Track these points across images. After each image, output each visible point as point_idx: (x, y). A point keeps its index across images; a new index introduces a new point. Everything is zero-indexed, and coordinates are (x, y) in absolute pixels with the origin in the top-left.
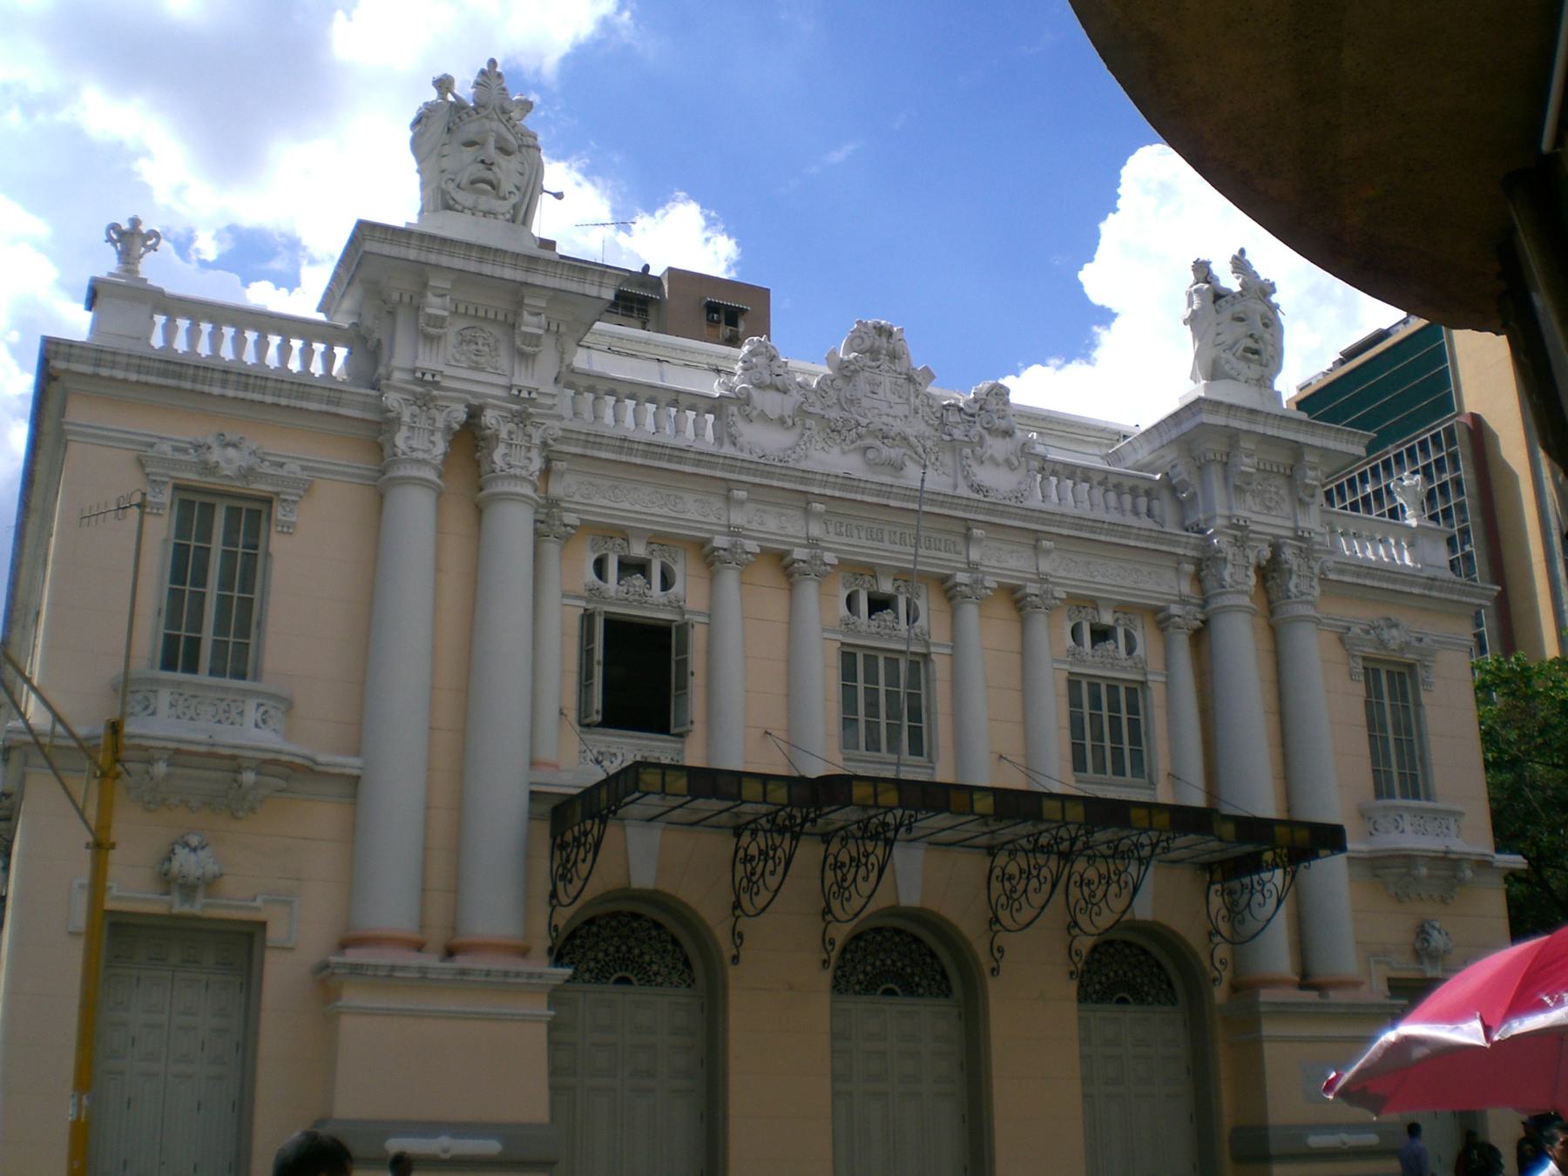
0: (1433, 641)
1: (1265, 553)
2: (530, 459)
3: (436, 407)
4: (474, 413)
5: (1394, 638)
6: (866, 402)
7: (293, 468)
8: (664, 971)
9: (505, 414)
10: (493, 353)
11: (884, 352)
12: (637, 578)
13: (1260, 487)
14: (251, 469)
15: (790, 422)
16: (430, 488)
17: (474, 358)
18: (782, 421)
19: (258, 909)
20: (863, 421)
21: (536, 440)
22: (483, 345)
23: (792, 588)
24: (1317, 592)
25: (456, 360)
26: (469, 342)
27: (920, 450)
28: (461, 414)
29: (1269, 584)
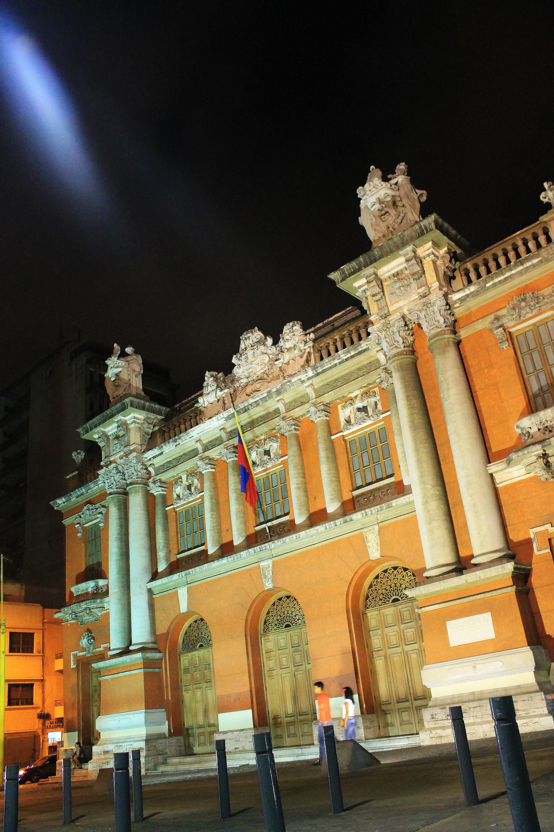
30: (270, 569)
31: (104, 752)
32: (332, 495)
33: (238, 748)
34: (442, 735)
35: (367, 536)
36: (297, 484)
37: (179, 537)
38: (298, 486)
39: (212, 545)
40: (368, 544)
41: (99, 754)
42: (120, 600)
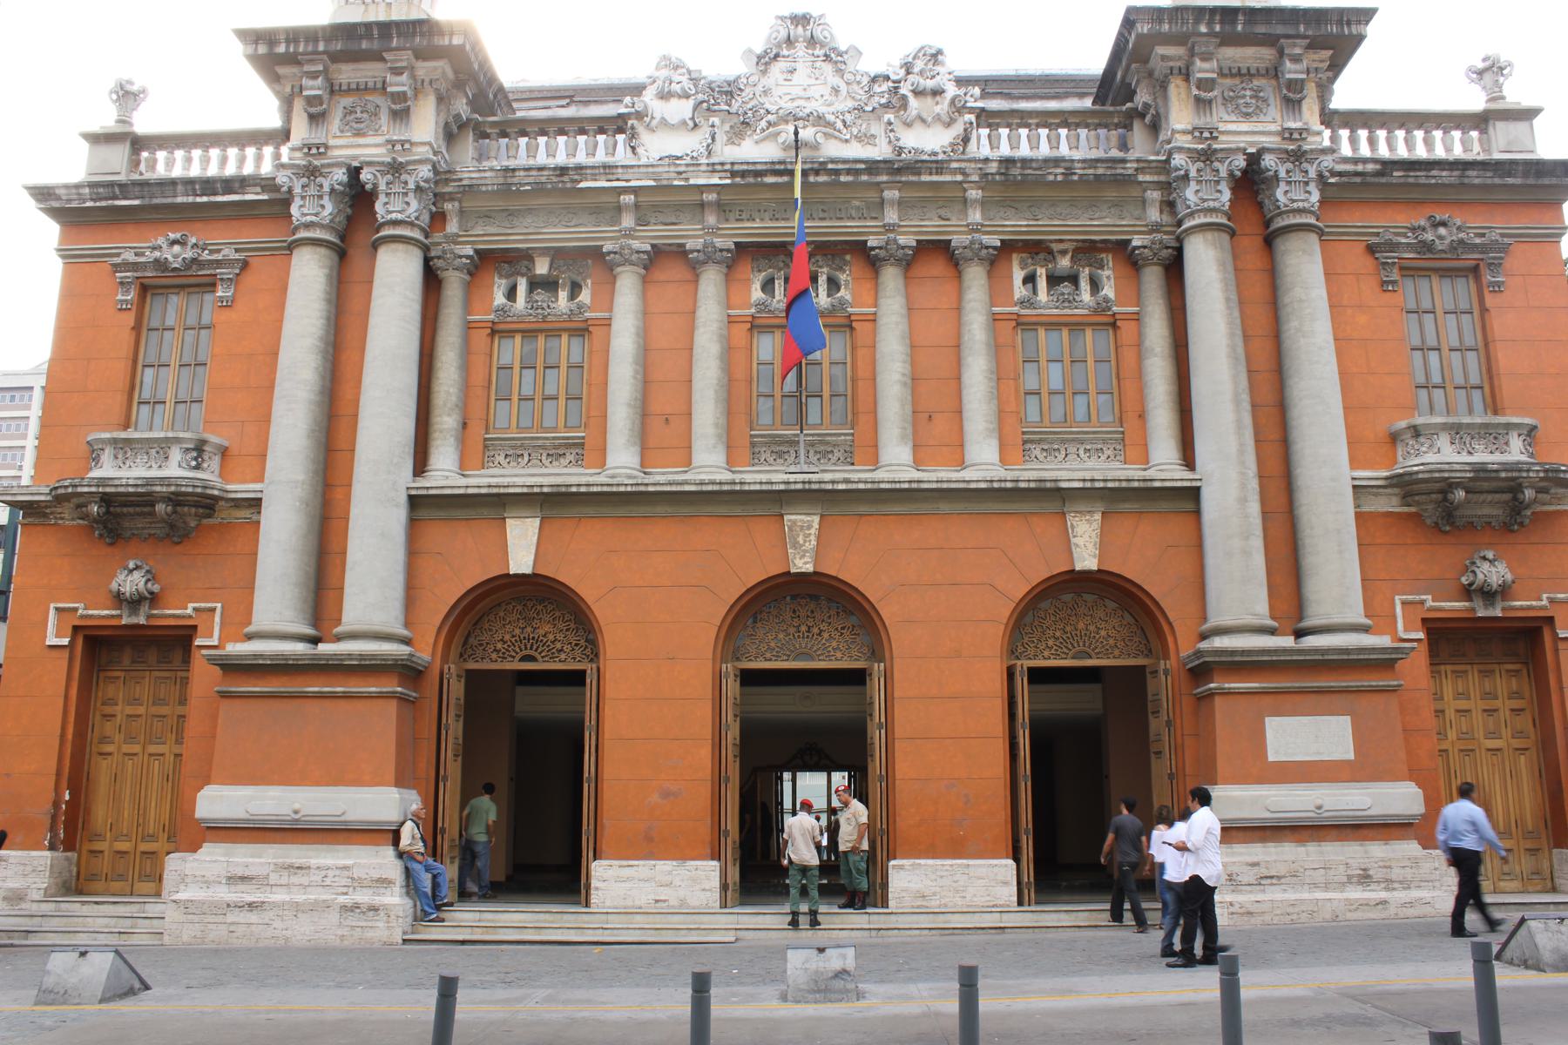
0: (1503, 235)
1: (1237, 163)
2: (408, 204)
3: (321, 175)
4: (354, 172)
5: (1441, 238)
6: (777, 92)
7: (229, 253)
8: (567, 648)
9: (382, 168)
10: (373, 118)
11: (801, 39)
12: (538, 294)
13: (1231, 94)
14: (194, 260)
15: (691, 124)
16: (321, 245)
17: (355, 126)
18: (684, 123)
19: (190, 617)
20: (773, 108)
21: (412, 186)
22: (362, 112)
23: (696, 280)
24: (1315, 197)
25: (342, 131)
26: (351, 112)
27: (839, 125)
28: (340, 175)
29: (1260, 198)
30: (813, 531)
31: (229, 878)
32: (991, 423)
33: (665, 901)
34: (1252, 910)
35: (1075, 523)
36: (904, 375)
37: (493, 397)
38: (905, 379)
39: (628, 441)
40: (1073, 540)
41: (206, 882)
42: (307, 505)
